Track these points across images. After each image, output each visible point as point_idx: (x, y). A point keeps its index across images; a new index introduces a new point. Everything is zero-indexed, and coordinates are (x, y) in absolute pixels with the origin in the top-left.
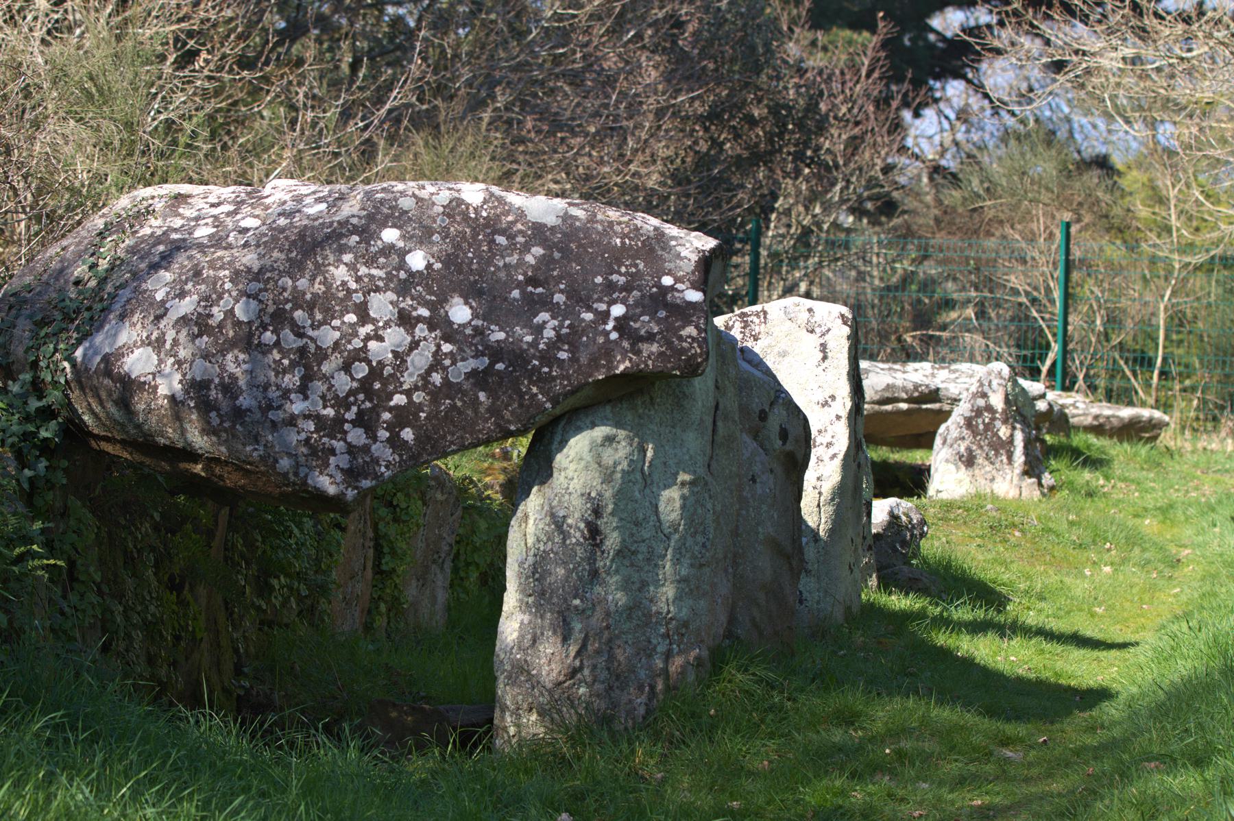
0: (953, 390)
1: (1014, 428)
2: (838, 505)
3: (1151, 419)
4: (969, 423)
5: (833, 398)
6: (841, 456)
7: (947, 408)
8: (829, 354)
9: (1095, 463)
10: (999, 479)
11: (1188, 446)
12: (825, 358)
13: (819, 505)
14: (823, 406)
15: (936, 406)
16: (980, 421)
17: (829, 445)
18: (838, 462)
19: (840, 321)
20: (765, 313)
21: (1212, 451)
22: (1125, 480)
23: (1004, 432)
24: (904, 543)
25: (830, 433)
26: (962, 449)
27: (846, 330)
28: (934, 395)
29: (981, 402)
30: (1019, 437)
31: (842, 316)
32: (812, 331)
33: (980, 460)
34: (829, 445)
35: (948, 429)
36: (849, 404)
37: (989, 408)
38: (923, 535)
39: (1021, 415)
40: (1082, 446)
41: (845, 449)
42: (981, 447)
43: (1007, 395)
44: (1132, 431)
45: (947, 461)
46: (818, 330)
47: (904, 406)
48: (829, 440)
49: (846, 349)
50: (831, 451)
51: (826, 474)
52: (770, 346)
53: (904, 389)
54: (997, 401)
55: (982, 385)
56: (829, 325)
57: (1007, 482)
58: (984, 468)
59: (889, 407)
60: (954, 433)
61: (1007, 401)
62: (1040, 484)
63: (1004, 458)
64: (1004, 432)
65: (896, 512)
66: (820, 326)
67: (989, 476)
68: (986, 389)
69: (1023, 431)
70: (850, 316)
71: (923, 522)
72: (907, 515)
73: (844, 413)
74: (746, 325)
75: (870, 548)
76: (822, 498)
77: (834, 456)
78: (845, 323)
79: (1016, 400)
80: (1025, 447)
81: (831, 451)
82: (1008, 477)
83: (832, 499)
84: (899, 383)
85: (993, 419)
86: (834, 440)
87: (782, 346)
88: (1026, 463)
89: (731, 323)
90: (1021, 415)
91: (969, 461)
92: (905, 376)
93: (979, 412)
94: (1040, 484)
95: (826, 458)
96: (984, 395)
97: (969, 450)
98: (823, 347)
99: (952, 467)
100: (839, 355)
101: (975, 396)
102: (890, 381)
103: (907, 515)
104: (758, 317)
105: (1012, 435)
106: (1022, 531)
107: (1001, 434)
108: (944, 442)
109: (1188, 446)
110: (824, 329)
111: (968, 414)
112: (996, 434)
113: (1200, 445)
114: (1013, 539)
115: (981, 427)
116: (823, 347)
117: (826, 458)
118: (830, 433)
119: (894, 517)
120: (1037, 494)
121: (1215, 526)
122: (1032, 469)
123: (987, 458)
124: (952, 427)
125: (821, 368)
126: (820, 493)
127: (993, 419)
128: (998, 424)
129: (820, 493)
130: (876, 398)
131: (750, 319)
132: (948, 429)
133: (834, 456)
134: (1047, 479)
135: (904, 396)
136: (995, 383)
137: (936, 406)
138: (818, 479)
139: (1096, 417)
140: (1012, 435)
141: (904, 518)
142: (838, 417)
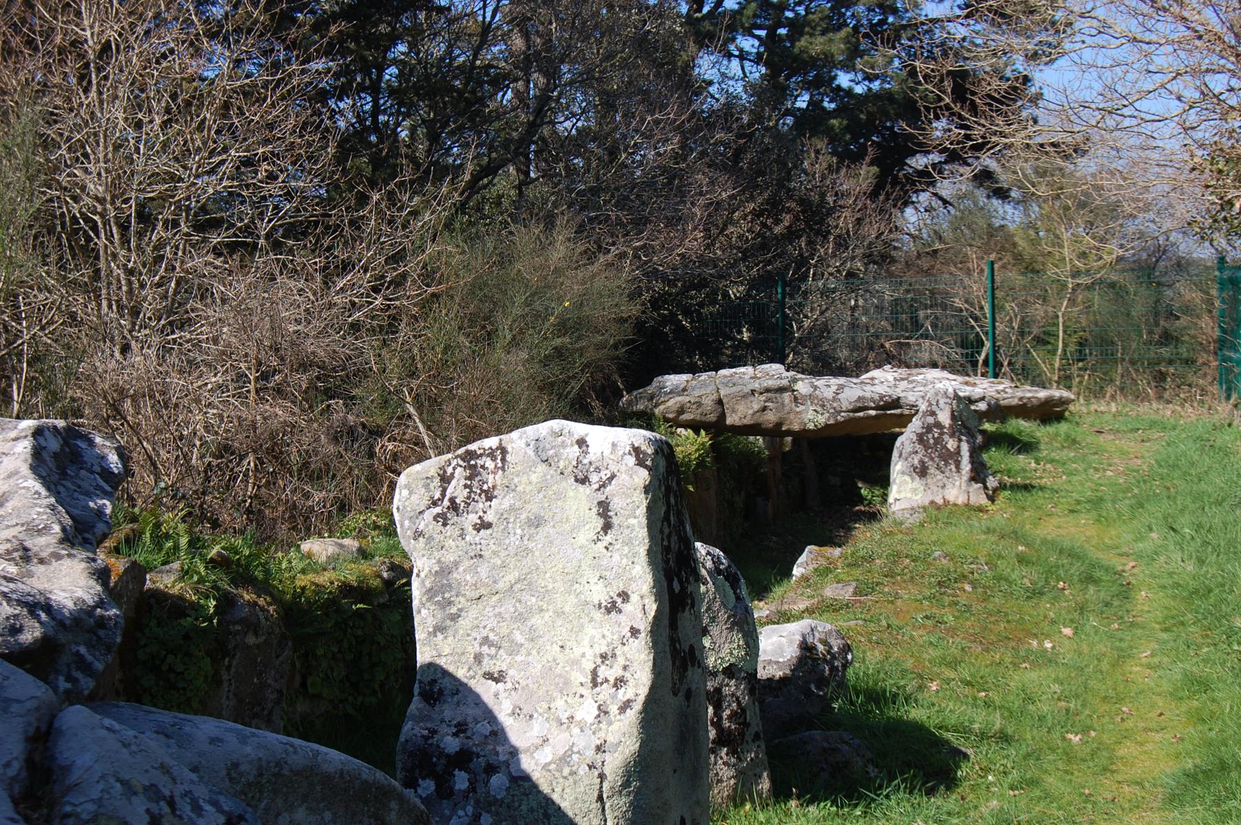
0: (911, 398)
1: (960, 440)
2: (638, 792)
3: (1061, 398)
4: (921, 439)
5: (625, 596)
6: (638, 706)
7: (907, 412)
8: (615, 521)
9: (1026, 447)
10: (949, 486)
11: (1084, 410)
12: (607, 527)
13: (600, 798)
14: (608, 611)
15: (898, 411)
16: (930, 436)
17: (619, 682)
18: (633, 715)
19: (631, 460)
20: (504, 451)
21: (1102, 413)
22: (1052, 461)
23: (951, 444)
24: (822, 682)
25: (621, 661)
26: (916, 462)
27: (643, 476)
28: (896, 403)
29: (931, 420)
30: (965, 448)
31: (636, 450)
32: (584, 481)
33: (932, 470)
34: (619, 682)
35: (902, 444)
36: (652, 608)
37: (938, 425)
38: (846, 665)
39: (966, 428)
40: (1015, 432)
41: (643, 691)
42: (932, 459)
43: (953, 412)
44: (1050, 413)
45: (903, 473)
46: (594, 478)
47: (873, 413)
48: (620, 673)
49: (642, 511)
50: (624, 694)
51: (611, 739)
52: (512, 509)
53: (872, 400)
54: (944, 418)
55: (930, 405)
56: (613, 468)
57: (956, 488)
58: (935, 475)
59: (861, 414)
60: (908, 448)
61: (953, 417)
62: (986, 488)
63: (953, 467)
64: (951, 444)
65: (810, 640)
66: (598, 470)
67: (940, 484)
68: (934, 408)
69: (968, 442)
70: (650, 451)
71: (847, 648)
72: (825, 642)
73: (644, 625)
74: (473, 473)
75: (757, 737)
76: (606, 785)
77: (626, 706)
78: (641, 463)
79: (961, 415)
80: (971, 456)
81: (624, 694)
82: (957, 483)
83: (626, 784)
84: (868, 395)
85: (942, 434)
86: (627, 675)
87: (534, 508)
88: (972, 470)
89: (449, 470)
90: (966, 428)
91: (922, 472)
92: (873, 388)
93: (929, 429)
94: (986, 488)
95: (614, 709)
96: (933, 414)
97: (922, 462)
98: (604, 508)
99: (907, 478)
100: (632, 521)
101: (924, 414)
102: (861, 394)
103: (825, 642)
104: (494, 459)
105: (959, 447)
106: (974, 584)
107: (949, 446)
108: (900, 456)
109: (1084, 410)
110: (605, 474)
111: (920, 431)
112: (945, 447)
113: (1093, 407)
114: (963, 600)
115: (932, 441)
116: (604, 508)
117: (614, 709)
118: (621, 661)
119: (806, 648)
120: (983, 501)
121: (1151, 529)
122: (979, 474)
123: (938, 468)
124: (907, 443)
125: (601, 545)
126: (602, 777)
127: (942, 434)
128: (946, 437)
129: (602, 777)
130: (851, 407)
131: (480, 462)
132: (902, 444)
133: (626, 706)
134: (992, 482)
135: (873, 405)
136: (942, 402)
137: (898, 411)
138: (599, 749)
139: (1021, 399)
140: (959, 447)
141: (821, 647)
142: (634, 632)
